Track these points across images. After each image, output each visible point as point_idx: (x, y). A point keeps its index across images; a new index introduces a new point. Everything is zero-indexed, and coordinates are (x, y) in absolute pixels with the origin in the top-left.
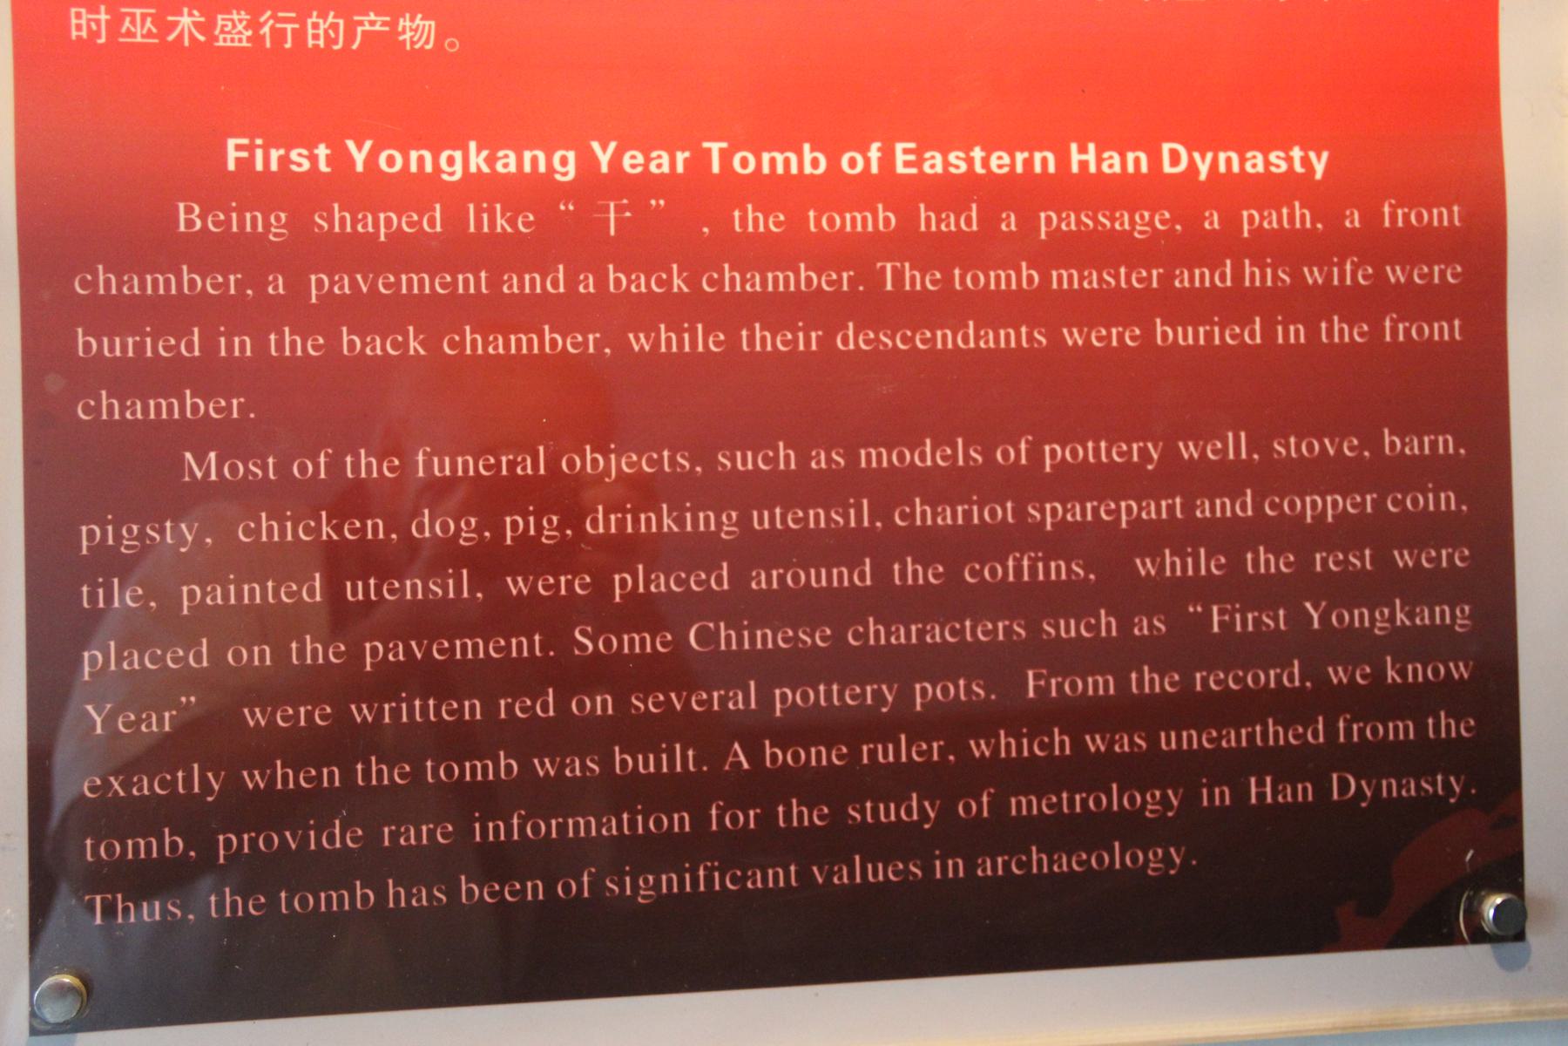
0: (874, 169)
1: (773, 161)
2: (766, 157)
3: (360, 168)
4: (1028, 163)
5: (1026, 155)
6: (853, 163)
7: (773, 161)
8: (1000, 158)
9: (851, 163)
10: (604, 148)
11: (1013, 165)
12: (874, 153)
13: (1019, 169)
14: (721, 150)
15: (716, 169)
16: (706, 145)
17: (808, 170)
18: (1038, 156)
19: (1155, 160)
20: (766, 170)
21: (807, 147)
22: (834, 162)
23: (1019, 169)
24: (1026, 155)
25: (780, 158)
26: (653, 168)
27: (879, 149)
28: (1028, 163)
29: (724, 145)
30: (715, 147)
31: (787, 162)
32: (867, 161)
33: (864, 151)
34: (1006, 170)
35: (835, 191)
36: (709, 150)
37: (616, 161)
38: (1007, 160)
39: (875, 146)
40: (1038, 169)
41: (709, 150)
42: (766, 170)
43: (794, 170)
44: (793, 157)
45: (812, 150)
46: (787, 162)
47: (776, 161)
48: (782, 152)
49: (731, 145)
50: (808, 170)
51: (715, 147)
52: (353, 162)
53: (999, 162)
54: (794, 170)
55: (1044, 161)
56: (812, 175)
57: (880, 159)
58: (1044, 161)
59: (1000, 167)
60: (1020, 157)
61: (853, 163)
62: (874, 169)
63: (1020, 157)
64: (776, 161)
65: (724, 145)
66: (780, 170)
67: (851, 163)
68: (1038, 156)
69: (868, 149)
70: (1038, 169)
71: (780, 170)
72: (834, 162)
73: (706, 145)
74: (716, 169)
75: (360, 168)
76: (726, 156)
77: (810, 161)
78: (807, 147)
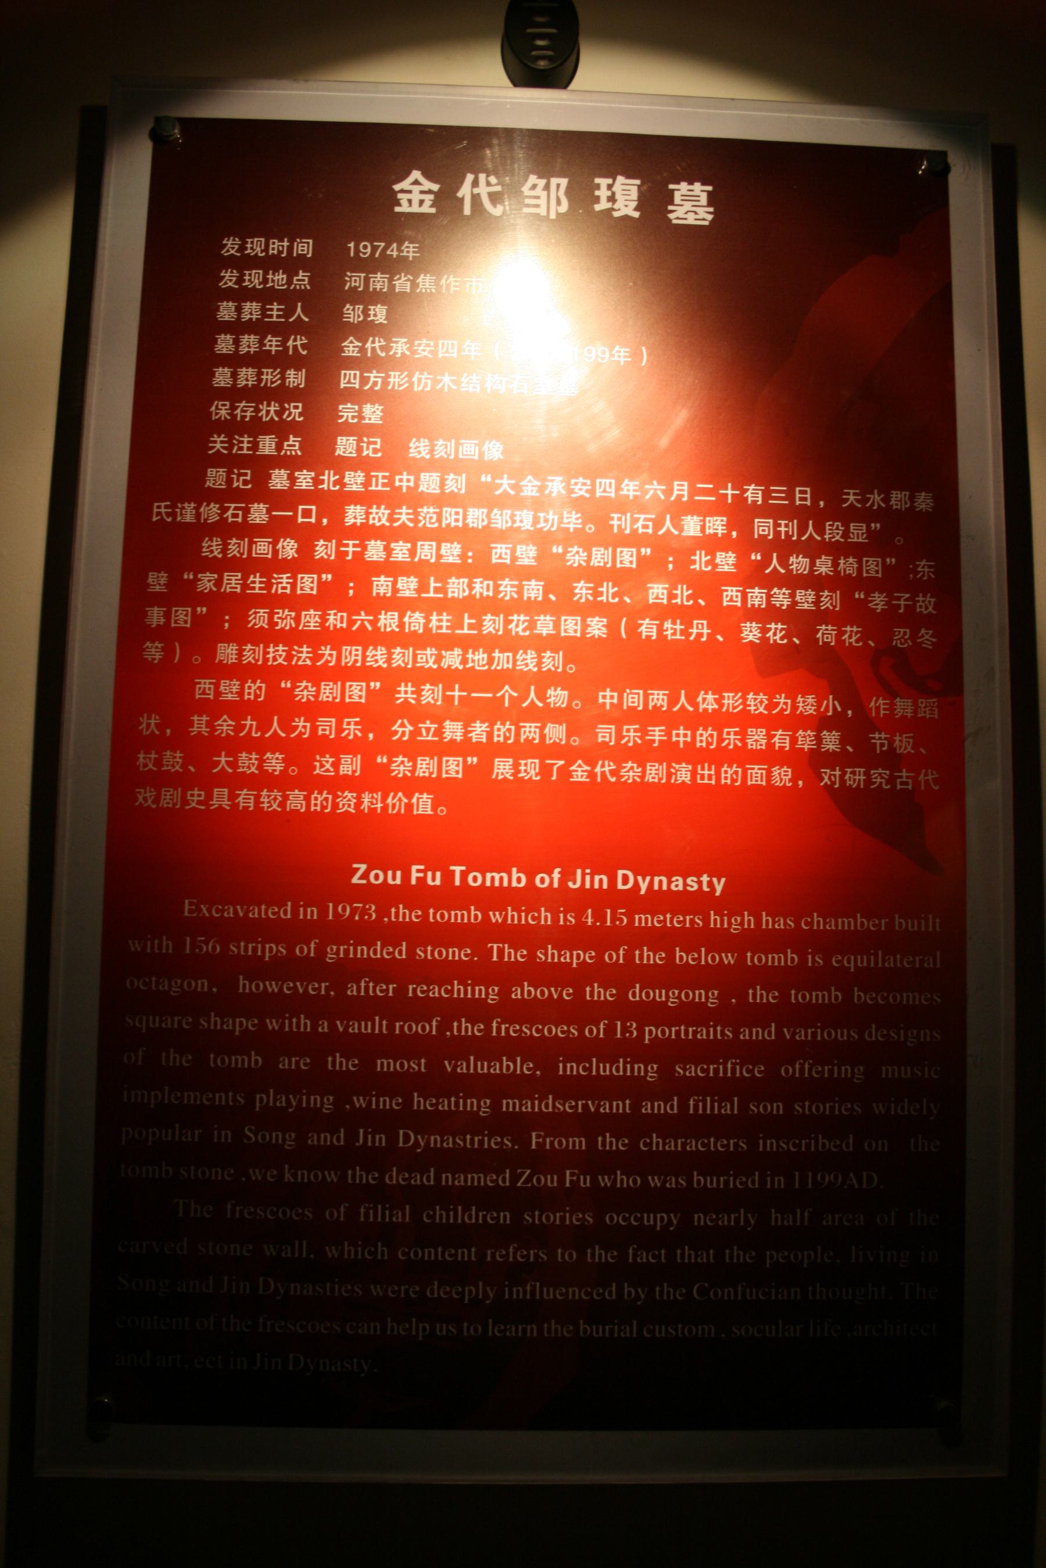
0: (556, 885)
1: (493, 878)
2: (489, 875)
6: (542, 881)
7: (493, 878)
9: (542, 881)
12: (556, 875)
14: (462, 871)
15: (457, 883)
16: (452, 868)
17: (514, 884)
19: (612, 881)
20: (488, 884)
21: (514, 870)
25: (497, 876)
29: (463, 868)
30: (458, 869)
31: (501, 879)
32: (552, 880)
33: (550, 873)
35: (529, 898)
36: (454, 871)
39: (558, 870)
41: (454, 871)
42: (488, 884)
43: (505, 884)
44: (505, 876)
45: (518, 872)
46: (501, 879)
47: (494, 878)
48: (499, 872)
50: (514, 884)
51: (458, 869)
54: (505, 884)
56: (516, 888)
61: (542, 881)
62: (556, 885)
64: (494, 878)
65: (463, 868)
66: (497, 884)
67: (542, 881)
69: (552, 872)
71: (497, 884)
73: (452, 868)
74: (457, 883)
76: (464, 875)
77: (517, 879)
78: (514, 870)
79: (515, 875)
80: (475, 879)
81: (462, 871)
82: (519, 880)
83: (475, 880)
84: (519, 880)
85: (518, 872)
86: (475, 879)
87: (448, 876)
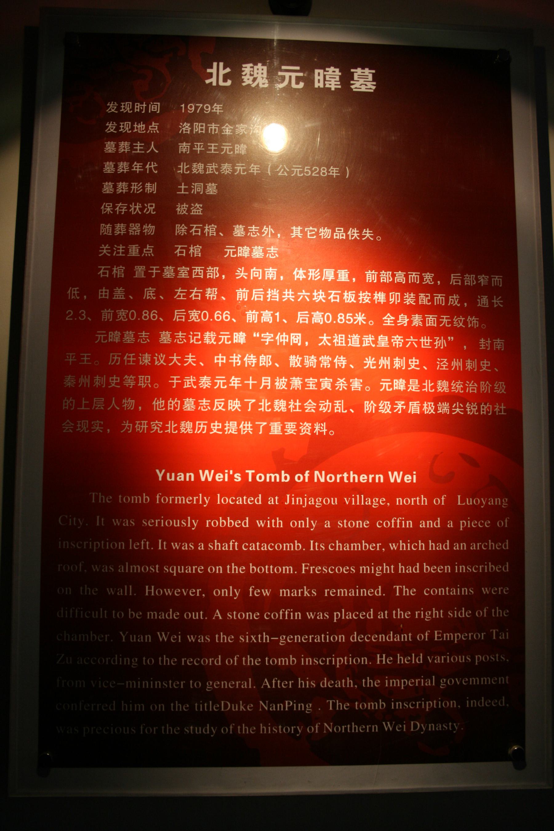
0: (307, 480)
1: (270, 477)
2: (268, 475)
3: (160, 479)
4: (374, 479)
5: (373, 476)
6: (299, 478)
7: (270, 477)
8: (364, 477)
9: (299, 478)
10: (160, 472)
11: (368, 479)
12: (307, 474)
13: (370, 481)
14: (252, 473)
15: (250, 480)
16: (247, 471)
17: (283, 480)
18: (377, 476)
20: (268, 480)
21: (283, 472)
22: (292, 478)
23: (370, 481)
24: (373, 476)
25: (273, 476)
26: (178, 479)
27: (308, 473)
28: (374, 479)
29: (253, 471)
30: (250, 472)
31: (275, 477)
32: (304, 477)
33: (303, 474)
34: (365, 481)
37: (164, 476)
38: (366, 477)
39: (307, 472)
40: (377, 481)
41: (248, 473)
42: (268, 480)
44: (278, 476)
45: (285, 473)
46: (275, 477)
47: (272, 477)
48: (274, 474)
49: (256, 471)
50: (283, 480)
51: (250, 472)
52: (158, 477)
53: (363, 478)
54: (278, 480)
55: (379, 478)
56: (284, 482)
57: (309, 477)
58: (379, 478)
59: (363, 480)
60: (371, 476)
61: (299, 478)
62: (307, 480)
63: (371, 476)
64: (272, 477)
65: (253, 471)
66: (273, 480)
67: (299, 478)
68: (377, 476)
70: (377, 481)
71: (273, 480)
72: (292, 478)
73: (247, 471)
74: (250, 480)
75: (160, 479)
76: (254, 476)
77: (285, 478)
78: (283, 472)
79: (283, 475)
80: (260, 478)
81: (252, 473)
82: (286, 478)
83: (260, 478)
84: (286, 478)
85: (285, 473)
86: (260, 478)
87: (245, 476)
